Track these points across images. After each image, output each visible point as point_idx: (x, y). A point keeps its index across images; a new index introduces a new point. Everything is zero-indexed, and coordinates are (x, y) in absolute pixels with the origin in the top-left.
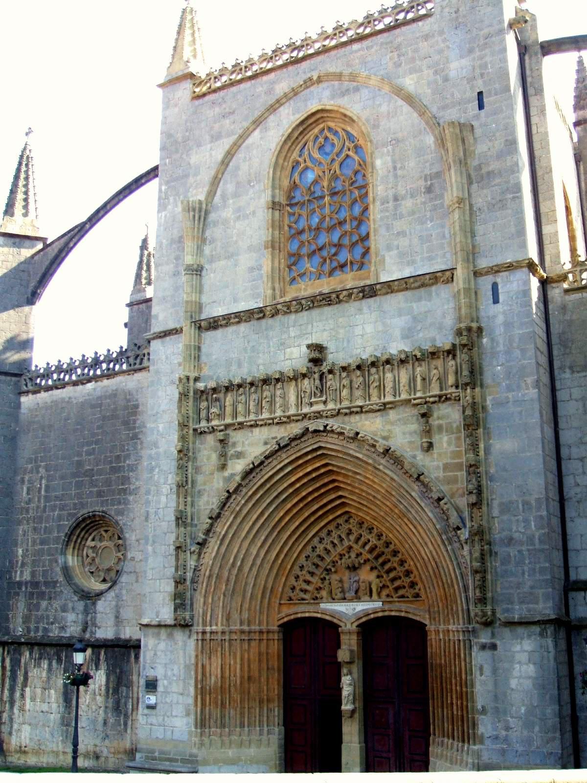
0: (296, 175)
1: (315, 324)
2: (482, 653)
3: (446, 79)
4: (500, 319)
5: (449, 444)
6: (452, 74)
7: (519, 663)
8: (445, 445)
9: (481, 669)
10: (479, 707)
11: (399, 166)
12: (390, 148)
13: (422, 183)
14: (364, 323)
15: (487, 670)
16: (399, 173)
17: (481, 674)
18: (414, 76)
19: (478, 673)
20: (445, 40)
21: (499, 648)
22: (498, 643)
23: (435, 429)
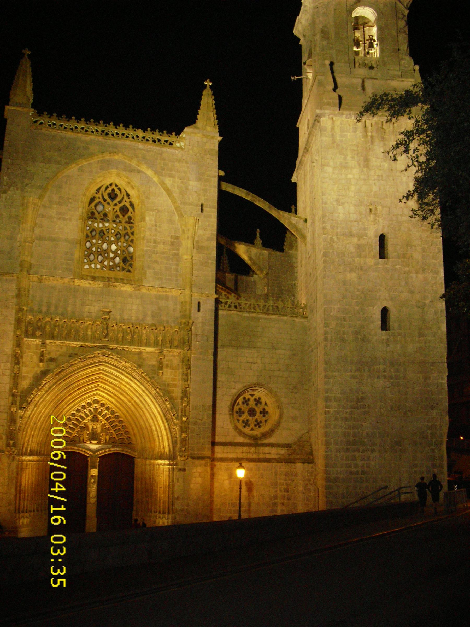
0: (93, 205)
1: (104, 296)
2: (179, 473)
3: (187, 189)
4: (200, 320)
5: (171, 374)
6: (190, 187)
7: (195, 477)
8: (169, 374)
9: (178, 479)
10: (176, 497)
11: (158, 225)
12: (154, 213)
13: (169, 239)
14: (132, 304)
15: (181, 480)
16: (158, 229)
17: (178, 482)
18: (171, 179)
19: (176, 481)
20: (188, 168)
21: (187, 470)
22: (186, 468)
23: (164, 366)
